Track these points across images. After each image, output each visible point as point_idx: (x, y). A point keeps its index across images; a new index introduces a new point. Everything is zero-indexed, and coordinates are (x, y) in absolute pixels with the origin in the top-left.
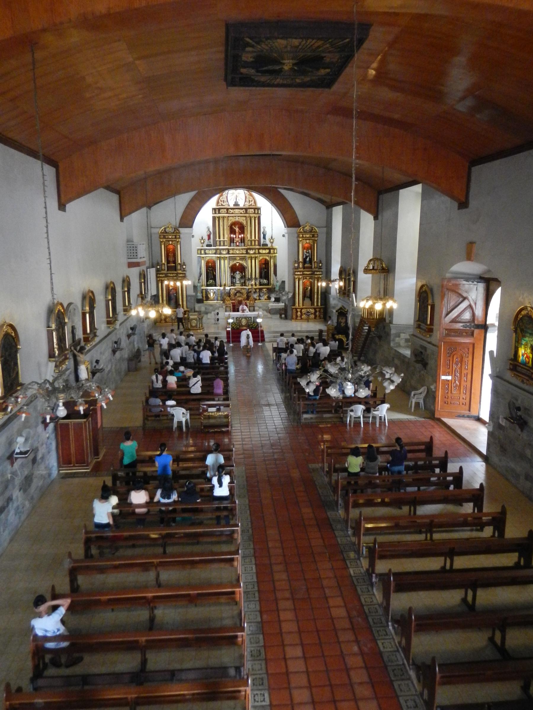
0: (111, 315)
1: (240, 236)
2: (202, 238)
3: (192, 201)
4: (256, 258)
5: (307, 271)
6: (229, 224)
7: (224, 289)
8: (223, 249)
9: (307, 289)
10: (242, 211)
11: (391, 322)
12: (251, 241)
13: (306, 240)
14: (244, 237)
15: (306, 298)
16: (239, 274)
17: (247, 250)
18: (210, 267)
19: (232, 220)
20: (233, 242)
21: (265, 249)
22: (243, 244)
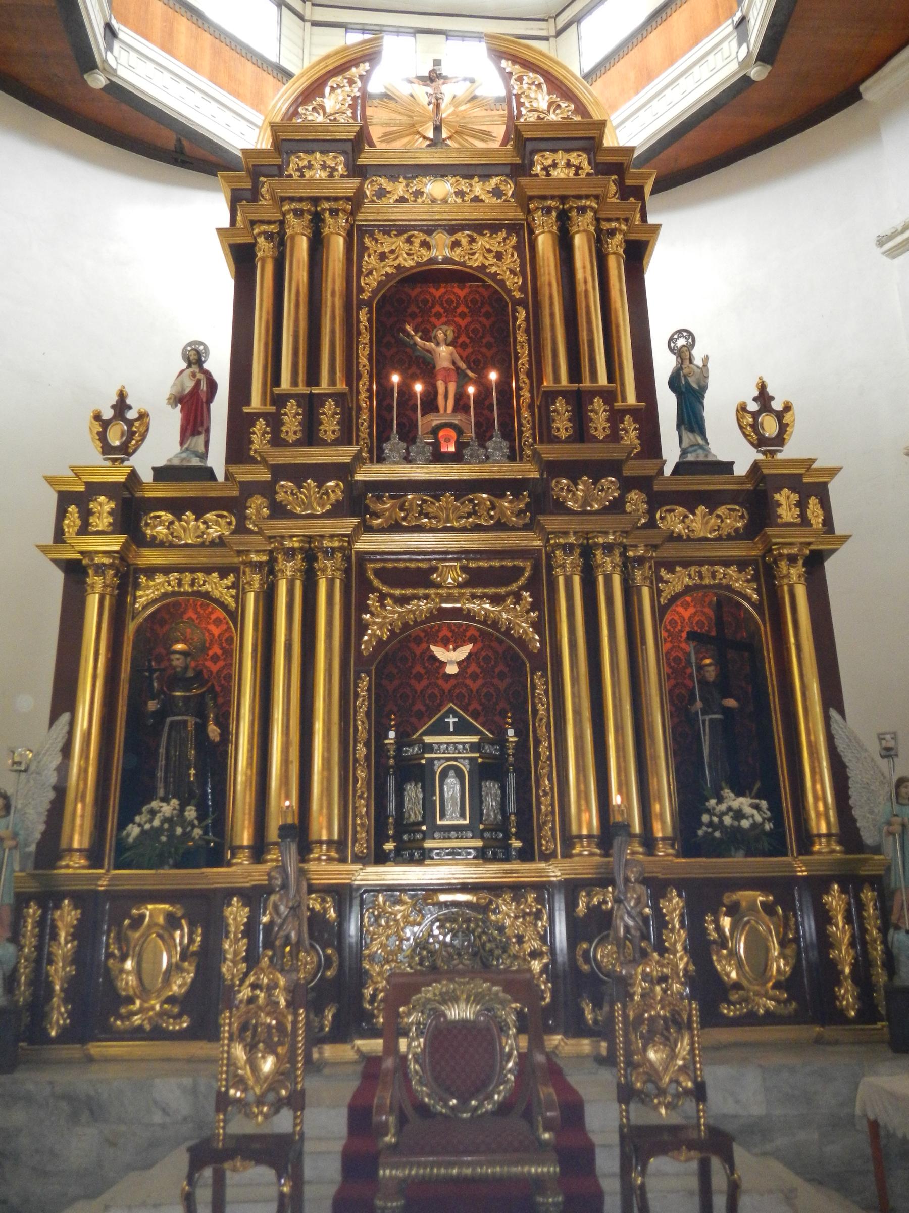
2: (121, 406)
8: (298, 474)
10: (478, 188)
14: (504, 386)
16: (463, 728)
18: (176, 680)
20: (408, 434)
21: (712, 500)
22: (497, 444)
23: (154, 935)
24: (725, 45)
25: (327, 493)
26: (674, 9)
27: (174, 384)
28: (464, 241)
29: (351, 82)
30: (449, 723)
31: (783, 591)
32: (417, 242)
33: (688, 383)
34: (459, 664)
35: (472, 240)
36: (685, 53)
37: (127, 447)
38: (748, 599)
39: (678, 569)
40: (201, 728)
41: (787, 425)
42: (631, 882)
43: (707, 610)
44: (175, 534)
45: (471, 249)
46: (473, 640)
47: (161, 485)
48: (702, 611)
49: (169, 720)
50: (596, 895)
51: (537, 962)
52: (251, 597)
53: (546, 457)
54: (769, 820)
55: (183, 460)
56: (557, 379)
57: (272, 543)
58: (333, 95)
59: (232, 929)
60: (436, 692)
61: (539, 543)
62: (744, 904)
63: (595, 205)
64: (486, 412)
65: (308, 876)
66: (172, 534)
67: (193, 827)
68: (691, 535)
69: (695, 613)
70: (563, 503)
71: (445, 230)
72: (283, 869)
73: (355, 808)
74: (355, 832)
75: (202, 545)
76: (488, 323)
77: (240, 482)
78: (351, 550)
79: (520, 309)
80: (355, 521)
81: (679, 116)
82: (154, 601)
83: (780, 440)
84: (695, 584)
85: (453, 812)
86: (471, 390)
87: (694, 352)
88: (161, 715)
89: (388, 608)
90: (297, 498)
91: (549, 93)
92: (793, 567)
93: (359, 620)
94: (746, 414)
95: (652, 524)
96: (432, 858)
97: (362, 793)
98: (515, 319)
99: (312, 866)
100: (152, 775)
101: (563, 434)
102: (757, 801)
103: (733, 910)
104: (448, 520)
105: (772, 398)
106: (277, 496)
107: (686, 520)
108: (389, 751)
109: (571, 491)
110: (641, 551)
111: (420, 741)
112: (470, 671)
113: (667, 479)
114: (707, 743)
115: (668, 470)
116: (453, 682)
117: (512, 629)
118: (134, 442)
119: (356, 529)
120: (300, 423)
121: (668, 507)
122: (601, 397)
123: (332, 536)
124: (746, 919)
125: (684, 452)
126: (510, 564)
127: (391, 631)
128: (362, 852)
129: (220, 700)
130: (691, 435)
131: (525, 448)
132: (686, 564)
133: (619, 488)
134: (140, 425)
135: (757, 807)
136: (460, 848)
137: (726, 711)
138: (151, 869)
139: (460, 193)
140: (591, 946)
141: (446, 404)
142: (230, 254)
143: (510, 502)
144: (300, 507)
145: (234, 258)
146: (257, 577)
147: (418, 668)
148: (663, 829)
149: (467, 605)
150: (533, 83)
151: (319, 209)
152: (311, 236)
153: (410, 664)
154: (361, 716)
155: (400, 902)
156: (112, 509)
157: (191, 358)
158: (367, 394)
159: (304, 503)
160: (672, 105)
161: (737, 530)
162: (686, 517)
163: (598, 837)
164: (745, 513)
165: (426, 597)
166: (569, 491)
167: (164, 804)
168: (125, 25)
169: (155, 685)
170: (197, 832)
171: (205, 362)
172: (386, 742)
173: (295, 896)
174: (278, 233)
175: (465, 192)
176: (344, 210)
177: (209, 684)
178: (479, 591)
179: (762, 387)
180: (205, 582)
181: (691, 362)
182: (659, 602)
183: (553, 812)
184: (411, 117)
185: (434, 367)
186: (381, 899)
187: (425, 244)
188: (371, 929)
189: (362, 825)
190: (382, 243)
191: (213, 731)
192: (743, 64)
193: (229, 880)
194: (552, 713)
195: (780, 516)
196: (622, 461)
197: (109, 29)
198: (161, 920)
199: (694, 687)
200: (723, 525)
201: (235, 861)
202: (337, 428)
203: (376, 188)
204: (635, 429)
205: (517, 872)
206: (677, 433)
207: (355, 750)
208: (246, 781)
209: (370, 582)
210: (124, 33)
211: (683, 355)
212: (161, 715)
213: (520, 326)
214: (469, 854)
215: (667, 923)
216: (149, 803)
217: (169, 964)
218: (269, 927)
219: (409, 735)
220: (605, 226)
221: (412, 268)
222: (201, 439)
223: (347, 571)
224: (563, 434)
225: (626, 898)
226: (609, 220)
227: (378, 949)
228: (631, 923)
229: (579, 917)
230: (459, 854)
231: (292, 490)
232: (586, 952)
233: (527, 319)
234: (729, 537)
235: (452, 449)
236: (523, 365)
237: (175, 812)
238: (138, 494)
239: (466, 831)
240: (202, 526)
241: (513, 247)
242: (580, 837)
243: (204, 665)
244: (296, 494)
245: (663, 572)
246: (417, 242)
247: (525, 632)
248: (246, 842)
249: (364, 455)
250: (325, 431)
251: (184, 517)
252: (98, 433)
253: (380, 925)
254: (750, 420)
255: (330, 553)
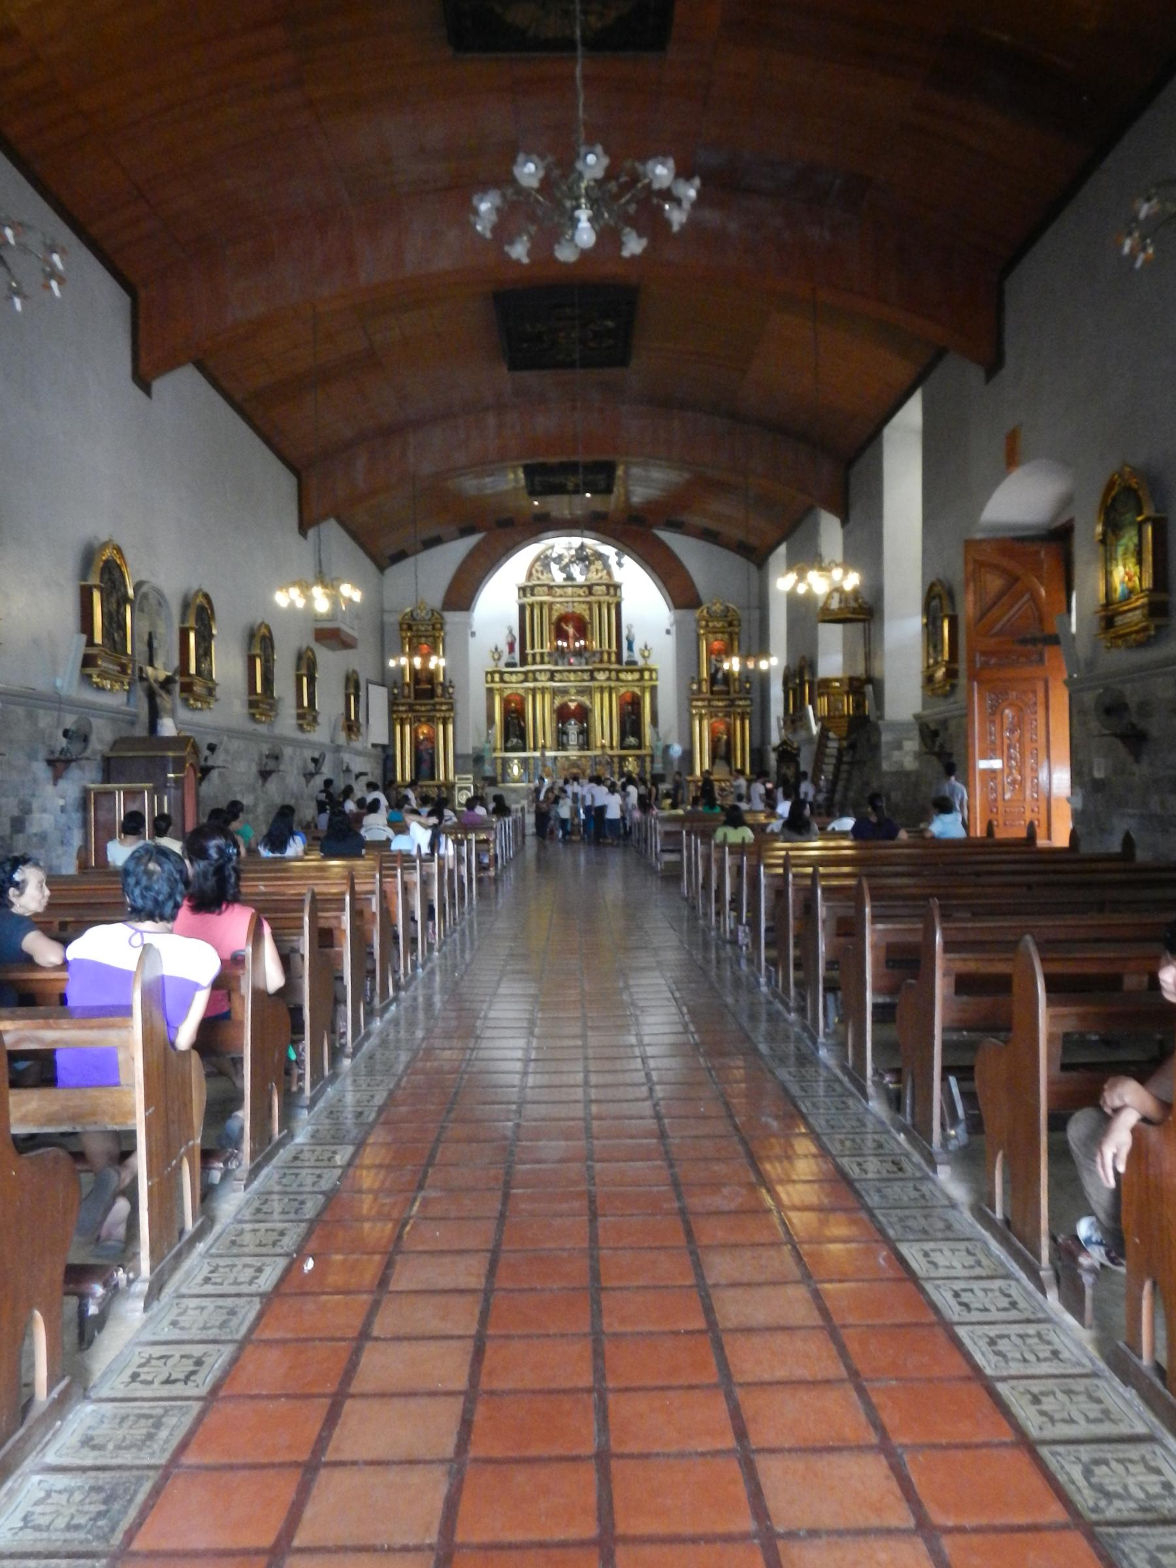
0: (259, 689)
1: (577, 645)
3: (473, 554)
4: (611, 689)
5: (719, 700)
6: (554, 617)
7: (543, 755)
8: (540, 671)
9: (719, 739)
10: (581, 592)
11: (881, 717)
12: (602, 653)
13: (715, 633)
15: (718, 761)
17: (592, 672)
18: (513, 712)
19: (560, 609)
21: (632, 671)
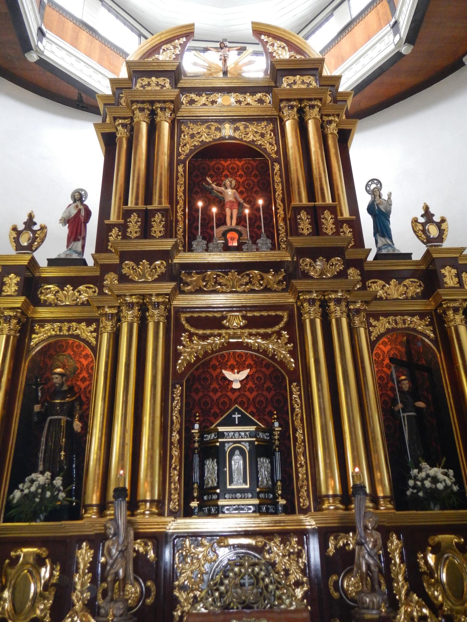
2: (30, 223)
6: (187, 149)
10: (249, 99)
14: (267, 207)
16: (244, 421)
18: (57, 393)
22: (263, 241)
23: (26, 571)
24: (386, 38)
25: (155, 268)
26: (355, 25)
27: (65, 212)
28: (241, 128)
29: (175, 47)
30: (235, 418)
31: (451, 331)
32: (213, 128)
33: (379, 209)
34: (241, 382)
35: (246, 127)
36: (362, 46)
37: (32, 246)
38: (428, 337)
39: (381, 318)
40: (70, 424)
41: (444, 230)
42: (368, 529)
43: (399, 347)
44: (59, 299)
45: (246, 132)
46: (249, 366)
47: (53, 269)
48: (395, 348)
49: (49, 418)
50: (341, 538)
51: (299, 590)
52: (105, 337)
53: (296, 245)
54: (455, 483)
55: (67, 255)
56: (300, 200)
57: (119, 299)
58: (164, 53)
59: (82, 566)
60: (226, 400)
61: (292, 300)
62: (443, 544)
63: (319, 104)
64: (256, 230)
65: (136, 526)
66: (57, 299)
67: (59, 490)
68: (389, 297)
69: (391, 349)
70: (308, 273)
71: (230, 121)
72: (115, 520)
73: (170, 477)
74: (170, 494)
75: (76, 305)
76: (256, 180)
77: (101, 265)
78: (171, 305)
79: (276, 164)
80: (173, 284)
81: (361, 77)
82: (43, 341)
83: (440, 238)
84: (393, 328)
85: (238, 479)
86: (247, 211)
87: (382, 192)
88: (43, 416)
89: (195, 342)
90: (136, 272)
91: (289, 51)
92: (457, 314)
93: (176, 350)
94: (417, 224)
95: (364, 287)
96: (224, 513)
97: (176, 466)
98: (273, 170)
99: (139, 519)
100: (37, 457)
101: (306, 232)
102: (446, 470)
103: (437, 550)
104: (233, 287)
105: (433, 215)
106: (123, 271)
107: (384, 288)
108: (195, 438)
109: (313, 266)
110: (358, 305)
111: (216, 430)
112: (248, 386)
113: (370, 262)
114: (407, 431)
115: (371, 258)
116: (237, 394)
117: (276, 355)
118: (36, 243)
119: (174, 289)
120: (139, 227)
121: (373, 280)
122: (329, 210)
123: (158, 295)
124: (445, 556)
125: (379, 249)
126: (273, 314)
127: (197, 357)
128: (175, 508)
129: (85, 407)
130: (383, 239)
131: (281, 244)
132: (386, 315)
133: (343, 264)
134: (41, 233)
135: (446, 474)
136: (243, 505)
137: (418, 410)
138: (27, 522)
139: (239, 102)
140: (339, 578)
141: (232, 222)
142: (102, 140)
143: (273, 276)
144: (138, 277)
145: (104, 142)
146: (110, 323)
147: (215, 385)
148: (384, 491)
149: (246, 340)
150: (280, 46)
151: (154, 108)
152: (149, 122)
153: (209, 382)
154: (176, 413)
155: (202, 545)
156: (18, 281)
157: (76, 197)
158: (182, 213)
159: (140, 275)
160: (357, 72)
161: (417, 294)
162: (384, 286)
163: (341, 496)
164: (422, 283)
165: (220, 335)
166: (311, 265)
167: (41, 476)
168: (50, 31)
169: (40, 394)
170: (62, 495)
171: (84, 201)
172: (193, 431)
173: (123, 542)
174: (129, 124)
175: (242, 101)
176: (169, 108)
177: (78, 395)
178: (254, 331)
179: (427, 209)
180: (76, 328)
181: (380, 197)
182: (370, 339)
183: (307, 479)
184: (210, 70)
185: (224, 201)
186: (188, 543)
187: (218, 129)
188: (180, 565)
189: (176, 489)
190: (192, 129)
191: (77, 426)
192: (397, 45)
193: (81, 530)
194: (304, 411)
195: (446, 283)
196: (344, 247)
197: (41, 33)
198: (31, 560)
199: (396, 395)
200: (408, 291)
201: (86, 515)
202: (162, 229)
203: (189, 99)
204: (350, 232)
205: (283, 522)
206: (374, 238)
207: (171, 436)
208: (97, 458)
209: (183, 326)
210: (49, 34)
211: (375, 193)
212: (43, 416)
213: (276, 173)
214: (250, 509)
215: (391, 559)
216: (30, 475)
217: (35, 593)
218: (104, 565)
219: (208, 427)
220: (326, 119)
221: (210, 142)
222: (79, 244)
223: (168, 318)
224: (306, 232)
225: (366, 542)
226: (328, 115)
227: (185, 581)
228: (371, 562)
229: (329, 556)
230: (243, 509)
231: (133, 267)
232: (336, 583)
233: (280, 169)
234: (412, 298)
235: (235, 244)
236: (279, 195)
237: (47, 481)
238: (37, 275)
239: (247, 493)
240: (77, 294)
241: (271, 130)
242: (327, 496)
243: (76, 384)
244: (135, 269)
245: (371, 320)
246: (213, 128)
247: (285, 357)
248: (94, 502)
249: (180, 248)
250: (155, 232)
251: (66, 288)
252: (14, 238)
253: (187, 563)
254: (421, 228)
255: (157, 305)
